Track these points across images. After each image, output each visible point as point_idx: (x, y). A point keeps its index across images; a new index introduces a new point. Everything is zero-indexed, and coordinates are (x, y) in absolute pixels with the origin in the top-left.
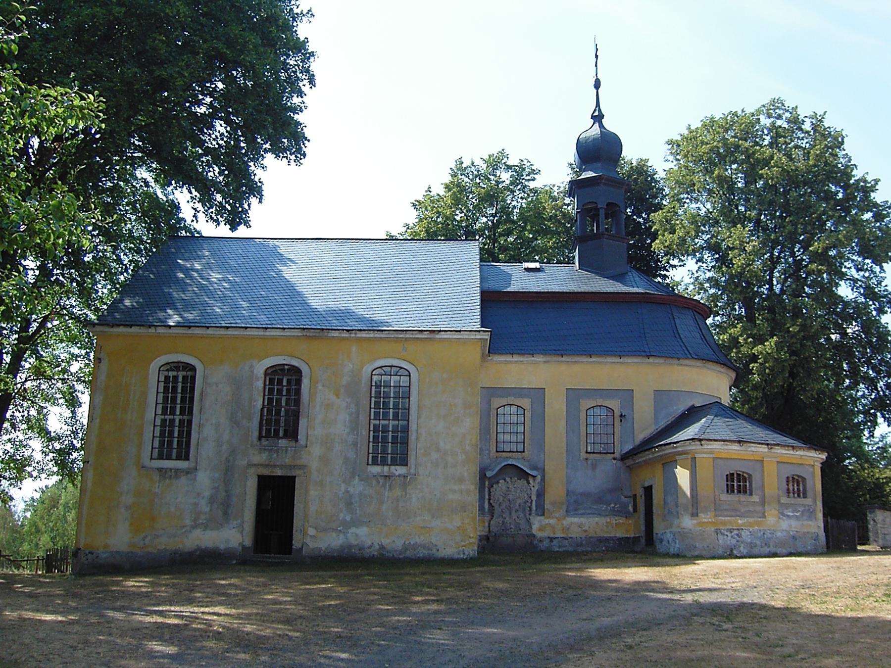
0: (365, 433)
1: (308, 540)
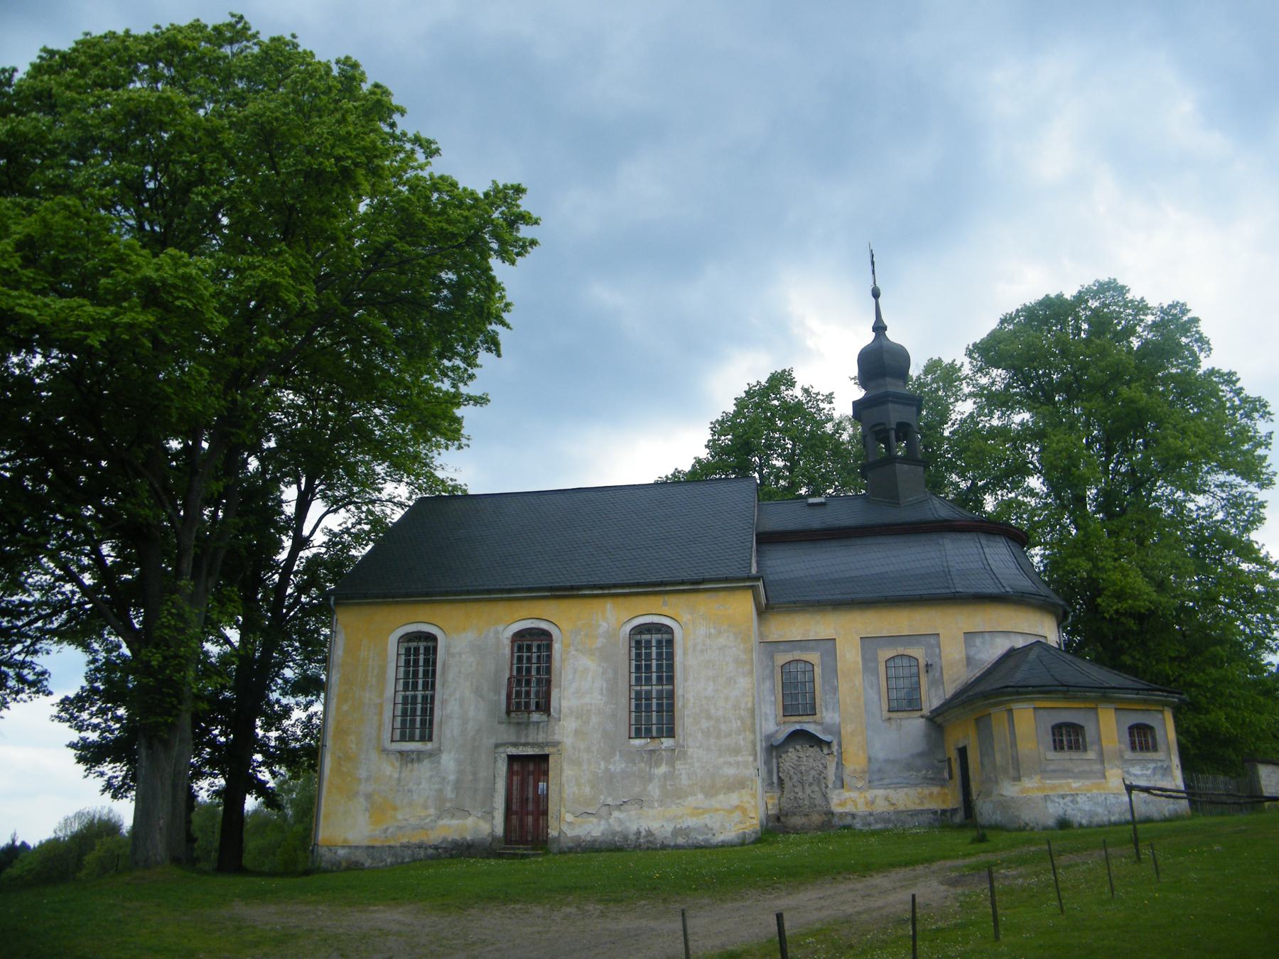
0: (624, 701)
1: (565, 828)
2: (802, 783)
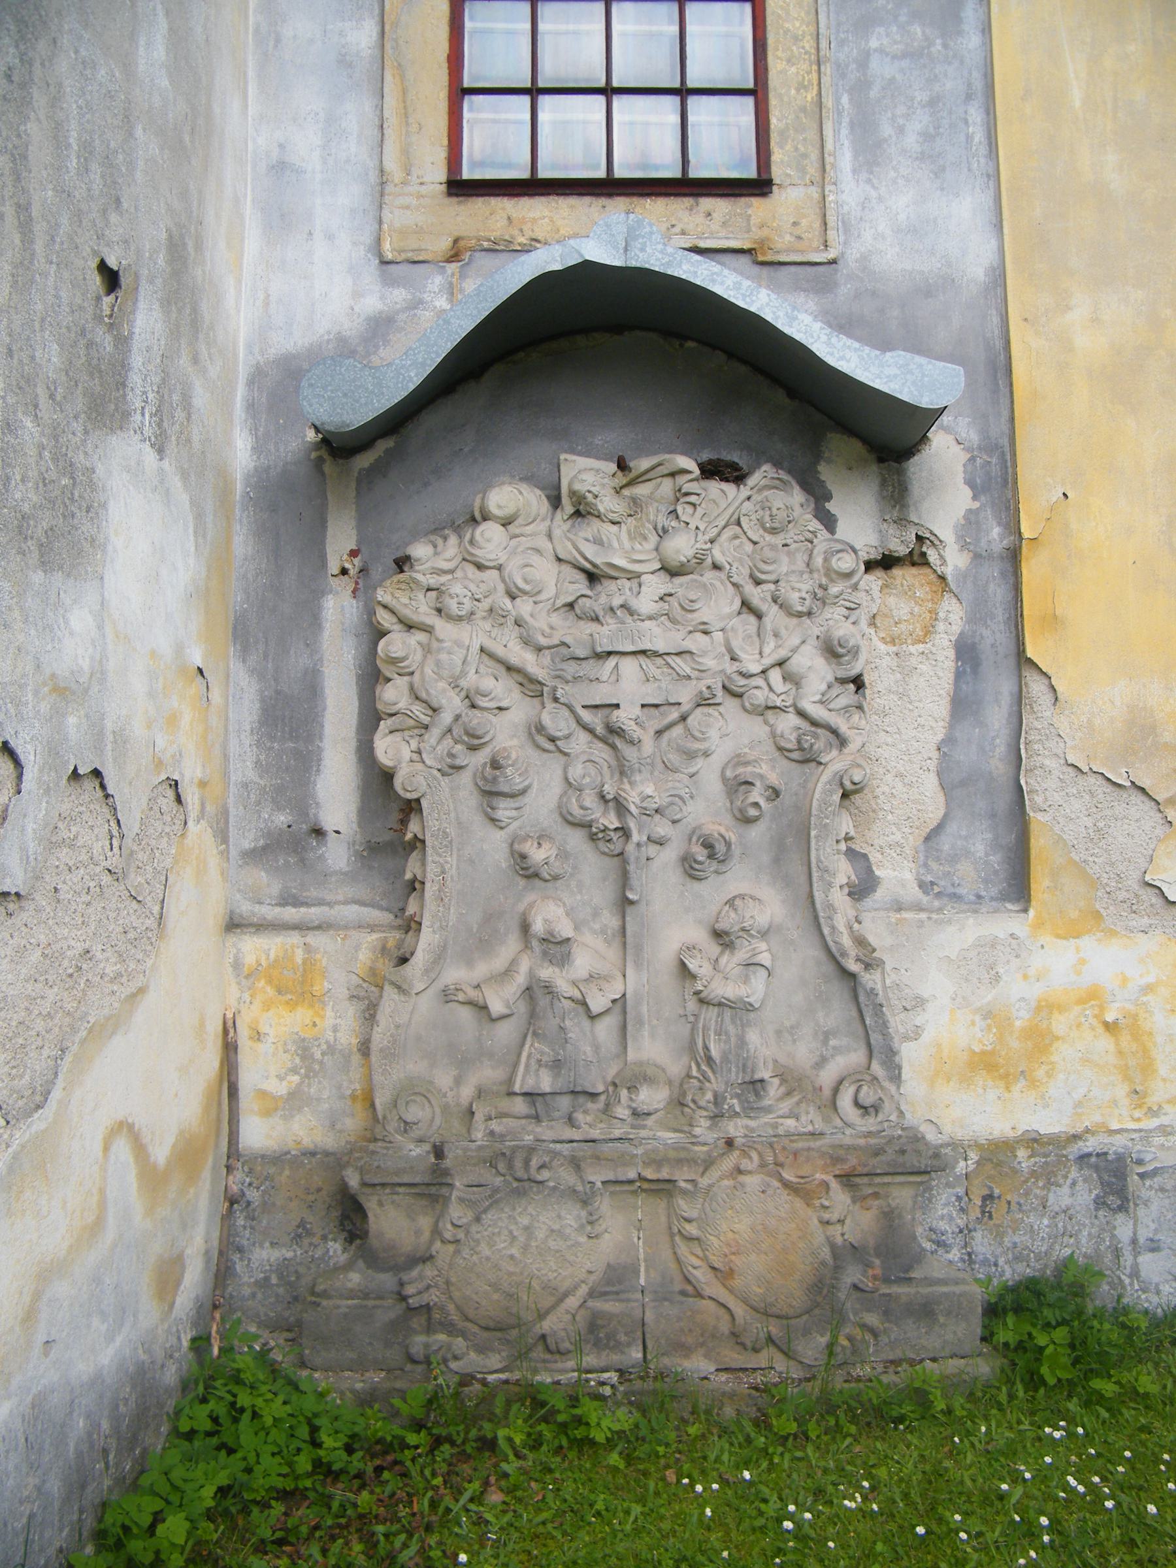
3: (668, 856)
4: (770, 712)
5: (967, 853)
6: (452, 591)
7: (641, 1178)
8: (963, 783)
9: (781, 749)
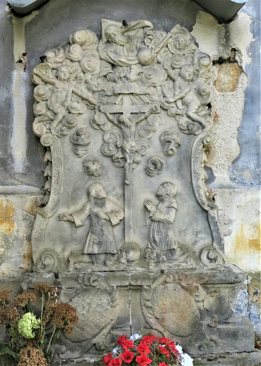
2: (120, 160)
3: (140, 168)
4: (177, 116)
5: (248, 168)
6: (62, 70)
7: (130, 285)
8: (246, 143)
9: (181, 129)
